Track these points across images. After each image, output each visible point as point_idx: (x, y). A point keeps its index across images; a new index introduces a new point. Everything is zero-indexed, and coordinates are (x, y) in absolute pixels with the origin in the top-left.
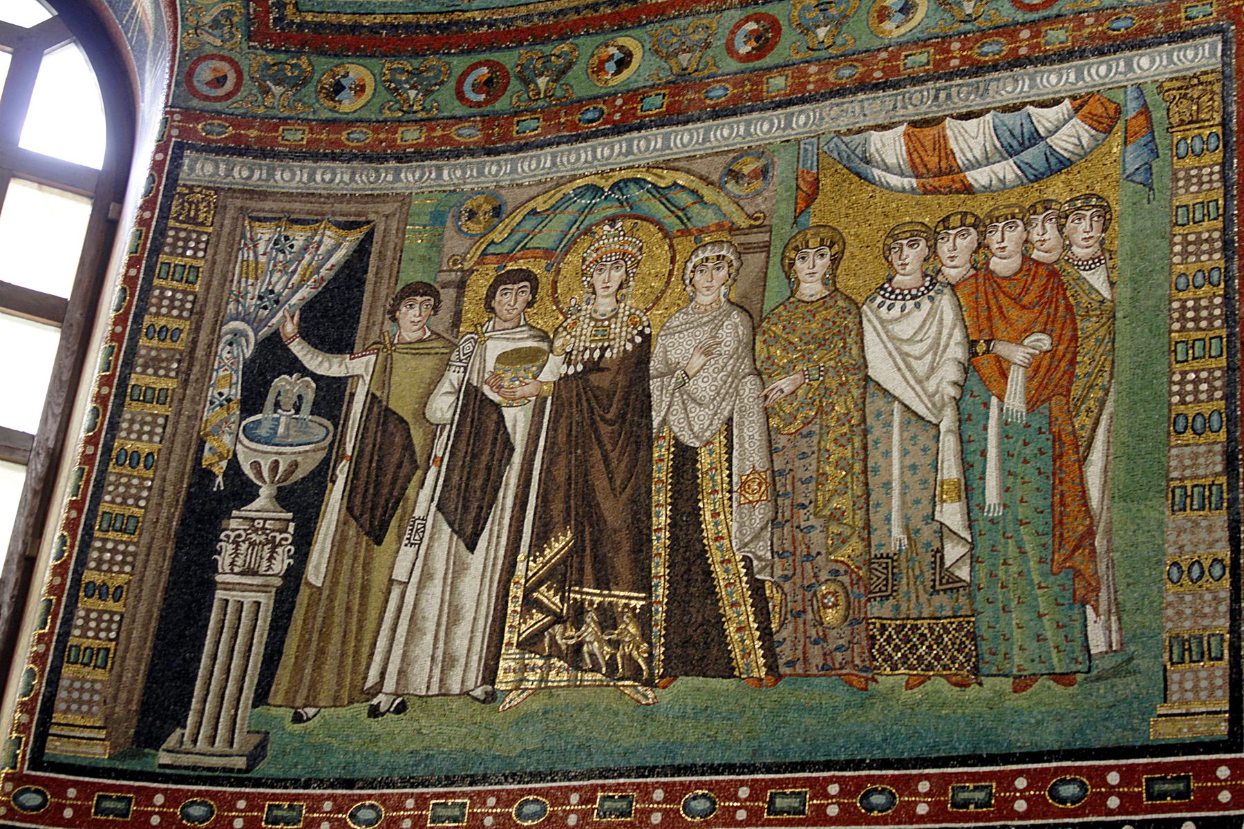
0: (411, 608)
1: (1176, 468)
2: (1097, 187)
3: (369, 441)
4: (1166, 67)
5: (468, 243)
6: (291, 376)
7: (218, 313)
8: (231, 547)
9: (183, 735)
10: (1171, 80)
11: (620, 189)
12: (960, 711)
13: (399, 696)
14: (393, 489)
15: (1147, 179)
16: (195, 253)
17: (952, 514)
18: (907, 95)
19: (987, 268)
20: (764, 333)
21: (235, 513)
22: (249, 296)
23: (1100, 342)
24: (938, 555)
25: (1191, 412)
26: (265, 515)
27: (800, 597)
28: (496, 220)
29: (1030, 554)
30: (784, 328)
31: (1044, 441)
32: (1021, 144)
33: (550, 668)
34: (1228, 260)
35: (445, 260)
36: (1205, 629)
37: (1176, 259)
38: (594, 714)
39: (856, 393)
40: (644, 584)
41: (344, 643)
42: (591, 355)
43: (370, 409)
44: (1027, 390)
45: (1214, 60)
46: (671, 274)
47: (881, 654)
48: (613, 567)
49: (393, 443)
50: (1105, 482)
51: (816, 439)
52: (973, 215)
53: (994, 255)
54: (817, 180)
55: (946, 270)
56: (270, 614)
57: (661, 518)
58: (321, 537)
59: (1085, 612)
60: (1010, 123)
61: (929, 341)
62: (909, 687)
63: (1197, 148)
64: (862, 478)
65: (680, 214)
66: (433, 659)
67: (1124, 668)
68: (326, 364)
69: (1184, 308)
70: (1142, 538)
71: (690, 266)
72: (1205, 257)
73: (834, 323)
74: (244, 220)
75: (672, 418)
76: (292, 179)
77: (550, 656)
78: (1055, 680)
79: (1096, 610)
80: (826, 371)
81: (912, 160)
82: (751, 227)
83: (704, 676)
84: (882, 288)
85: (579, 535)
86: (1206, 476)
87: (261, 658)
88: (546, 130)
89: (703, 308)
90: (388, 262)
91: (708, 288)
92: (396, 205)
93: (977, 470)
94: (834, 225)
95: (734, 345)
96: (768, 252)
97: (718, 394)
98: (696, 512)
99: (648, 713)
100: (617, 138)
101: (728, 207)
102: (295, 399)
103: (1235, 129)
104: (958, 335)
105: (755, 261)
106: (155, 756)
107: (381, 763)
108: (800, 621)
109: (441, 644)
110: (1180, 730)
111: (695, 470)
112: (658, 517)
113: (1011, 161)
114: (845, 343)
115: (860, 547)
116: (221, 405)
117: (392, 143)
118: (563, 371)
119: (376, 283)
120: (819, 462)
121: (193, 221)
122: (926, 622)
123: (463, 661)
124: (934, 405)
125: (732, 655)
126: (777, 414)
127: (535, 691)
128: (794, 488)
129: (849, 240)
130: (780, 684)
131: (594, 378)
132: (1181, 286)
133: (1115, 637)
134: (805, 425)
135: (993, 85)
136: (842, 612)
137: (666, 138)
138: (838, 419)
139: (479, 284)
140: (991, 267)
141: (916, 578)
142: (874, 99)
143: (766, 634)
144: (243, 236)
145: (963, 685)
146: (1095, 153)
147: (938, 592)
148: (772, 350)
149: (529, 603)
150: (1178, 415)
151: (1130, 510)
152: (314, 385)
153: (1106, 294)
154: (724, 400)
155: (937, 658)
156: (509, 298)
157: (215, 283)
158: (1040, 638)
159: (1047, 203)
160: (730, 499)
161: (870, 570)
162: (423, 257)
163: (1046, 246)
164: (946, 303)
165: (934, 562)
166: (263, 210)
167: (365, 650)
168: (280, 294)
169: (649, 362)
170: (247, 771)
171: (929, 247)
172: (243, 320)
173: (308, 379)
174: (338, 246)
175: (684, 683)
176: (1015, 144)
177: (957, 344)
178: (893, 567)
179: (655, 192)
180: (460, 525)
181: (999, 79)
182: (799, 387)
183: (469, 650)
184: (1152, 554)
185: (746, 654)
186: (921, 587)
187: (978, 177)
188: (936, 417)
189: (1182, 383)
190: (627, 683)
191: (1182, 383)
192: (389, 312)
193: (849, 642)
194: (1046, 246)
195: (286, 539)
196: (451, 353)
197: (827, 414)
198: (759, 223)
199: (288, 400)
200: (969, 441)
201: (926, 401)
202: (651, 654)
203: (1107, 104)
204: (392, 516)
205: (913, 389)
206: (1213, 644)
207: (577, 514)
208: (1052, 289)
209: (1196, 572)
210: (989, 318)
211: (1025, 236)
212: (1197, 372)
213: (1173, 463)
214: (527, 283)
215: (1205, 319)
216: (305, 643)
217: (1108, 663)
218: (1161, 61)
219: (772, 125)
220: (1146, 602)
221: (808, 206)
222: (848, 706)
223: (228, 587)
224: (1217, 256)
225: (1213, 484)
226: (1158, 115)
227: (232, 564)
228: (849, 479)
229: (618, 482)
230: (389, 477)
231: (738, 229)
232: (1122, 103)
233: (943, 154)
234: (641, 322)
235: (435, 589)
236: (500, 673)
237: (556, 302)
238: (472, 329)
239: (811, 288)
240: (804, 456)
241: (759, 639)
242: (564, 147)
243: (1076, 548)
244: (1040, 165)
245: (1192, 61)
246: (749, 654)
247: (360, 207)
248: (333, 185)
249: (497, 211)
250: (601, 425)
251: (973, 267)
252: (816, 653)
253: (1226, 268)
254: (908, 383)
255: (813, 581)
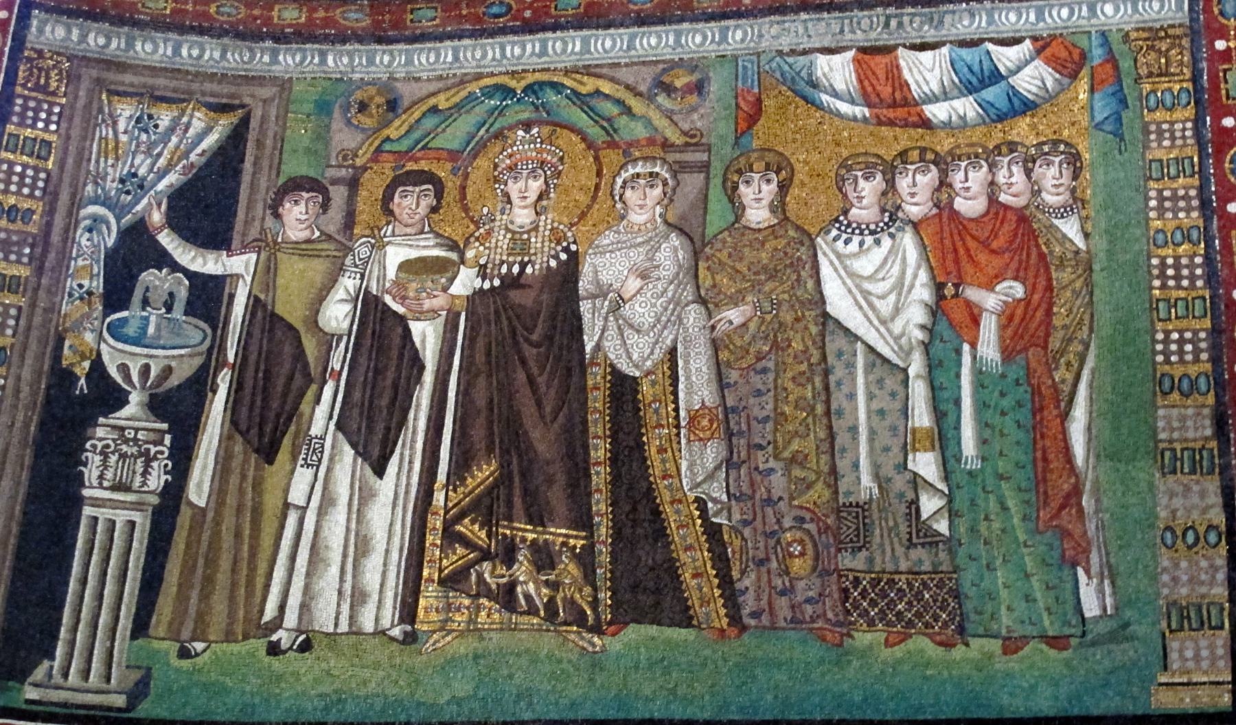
0: (311, 535)
1: (1164, 430)
2: (1066, 133)
3: (254, 348)
4: (1131, 16)
5: (360, 137)
6: (160, 270)
7: (73, 195)
8: (98, 458)
9: (52, 667)
10: (1137, 30)
11: (535, 92)
12: (946, 673)
13: (302, 633)
14: (284, 402)
15: (1118, 129)
16: (47, 126)
17: (926, 464)
18: (855, 20)
19: (951, 207)
20: (708, 259)
21: (101, 420)
22: (109, 178)
23: (1076, 294)
24: (913, 507)
25: (1178, 372)
26: (137, 424)
27: (761, 545)
28: (391, 115)
29: (1013, 510)
30: (730, 255)
31: (1023, 393)
32: (981, 81)
33: (478, 608)
34: (1207, 220)
35: (334, 155)
36: (1203, 596)
37: (1152, 214)
38: (534, 661)
39: (814, 330)
40: (584, 522)
41: (234, 571)
42: (510, 269)
43: (253, 315)
44: (1002, 339)
45: (1180, 14)
46: (597, 187)
47: (856, 608)
48: (548, 503)
49: (280, 353)
50: (1090, 440)
51: (771, 376)
52: (933, 151)
53: (957, 195)
54: (759, 101)
55: (907, 207)
56: (146, 535)
57: (600, 450)
58: (202, 452)
59: (1076, 574)
60: (968, 59)
61: (892, 280)
62: (887, 644)
63: (1168, 103)
64: (825, 421)
65: (605, 124)
66: (340, 592)
67: (1120, 632)
68: (200, 260)
69: (1163, 265)
70: (1133, 500)
71: (619, 181)
72: (1181, 215)
73: (786, 254)
74: (101, 93)
75: (607, 344)
76: (155, 51)
77: (478, 596)
78: (1048, 644)
79: (1087, 572)
80: (780, 304)
81: (863, 88)
82: (687, 144)
83: (659, 624)
84: (837, 220)
85: (504, 466)
86: (1195, 440)
87: (138, 585)
88: (443, 24)
89: (636, 228)
90: (268, 151)
91: (641, 207)
92: (274, 89)
93: (951, 418)
94: (781, 149)
95: (674, 270)
96: (708, 173)
97: (659, 321)
98: (640, 446)
99: (596, 662)
100: (528, 37)
101: (660, 122)
102: (166, 297)
103: (1206, 85)
104: (923, 276)
105: (693, 182)
106: (20, 690)
107: (283, 705)
108: (764, 569)
109: (349, 577)
110: (1182, 700)
111: (635, 401)
112: (596, 450)
113: (971, 98)
114: (799, 276)
115: (827, 494)
116: (81, 298)
117: (268, 21)
118: (478, 283)
119: (254, 174)
120: (776, 400)
121: (44, 89)
122: (903, 577)
123: (375, 597)
124: (901, 347)
125: (690, 603)
126: (727, 347)
127: (462, 634)
128: (749, 429)
129: (798, 167)
130: (745, 636)
131: (515, 296)
132: (1160, 242)
133: (1109, 601)
134: (759, 359)
135: (948, 19)
136: (810, 562)
137: (585, 42)
138: (795, 357)
139: (373, 184)
140: (956, 206)
141: (890, 530)
142: (818, 19)
143: (726, 582)
144: (101, 110)
145: (948, 645)
146: (1062, 97)
147: (915, 546)
148: (718, 277)
149: (451, 536)
150: (1163, 375)
151: (1118, 470)
152: (187, 283)
153: (1080, 243)
154: (665, 327)
155: (919, 615)
156: (410, 201)
157: (70, 161)
158: (1028, 598)
159: (1012, 147)
160: (678, 435)
161: (839, 518)
162: (308, 151)
163: (1014, 189)
164: (908, 240)
165: (910, 514)
166: (123, 84)
167: (260, 581)
168: (144, 179)
169: (577, 282)
170: (127, 710)
171: (887, 182)
172: (103, 204)
173: (181, 275)
174: (208, 130)
175: (633, 632)
176: (974, 80)
177: (922, 285)
178: (864, 517)
179: (575, 99)
180: (365, 447)
181: (954, 12)
182: (750, 320)
183: (382, 585)
184: (1143, 516)
185: (704, 602)
186: (896, 540)
187: (936, 111)
188: (904, 361)
189: (1166, 341)
190: (569, 628)
191: (1166, 341)
192: (270, 207)
193: (820, 595)
194: (1014, 189)
195: (162, 453)
196: (345, 256)
197: (783, 350)
198: (694, 140)
199: (158, 297)
200: (941, 389)
201: (892, 342)
202: (596, 599)
203: (1071, 48)
204: (284, 434)
205: (877, 330)
206: (1214, 612)
207: (501, 441)
208: (1023, 235)
209: (1190, 538)
210: (957, 261)
211: (990, 178)
212: (1181, 332)
213: (1161, 424)
214: (430, 187)
215: (1186, 278)
216: (188, 569)
217: (1102, 628)
218: (1126, 10)
219: (705, 38)
220: (1140, 567)
221: (750, 127)
222: (822, 661)
223: (97, 503)
224: (1195, 214)
225: (1203, 447)
226: (1125, 64)
227: (101, 477)
228: (810, 420)
229: (548, 409)
230: (279, 389)
231: (672, 145)
232: (1086, 49)
233: (897, 85)
234: (566, 239)
235: (338, 518)
236: (421, 613)
237: (466, 209)
238: (367, 232)
239: (758, 215)
240: (759, 393)
241: (719, 587)
242: (466, 42)
243: (1062, 507)
244: (1003, 104)
245: (1159, 12)
246: (709, 603)
247: (233, 89)
248: (202, 62)
249: (392, 105)
250: (525, 346)
251: (935, 205)
252: (782, 603)
253: (1205, 229)
254: (871, 323)
255: (776, 527)
